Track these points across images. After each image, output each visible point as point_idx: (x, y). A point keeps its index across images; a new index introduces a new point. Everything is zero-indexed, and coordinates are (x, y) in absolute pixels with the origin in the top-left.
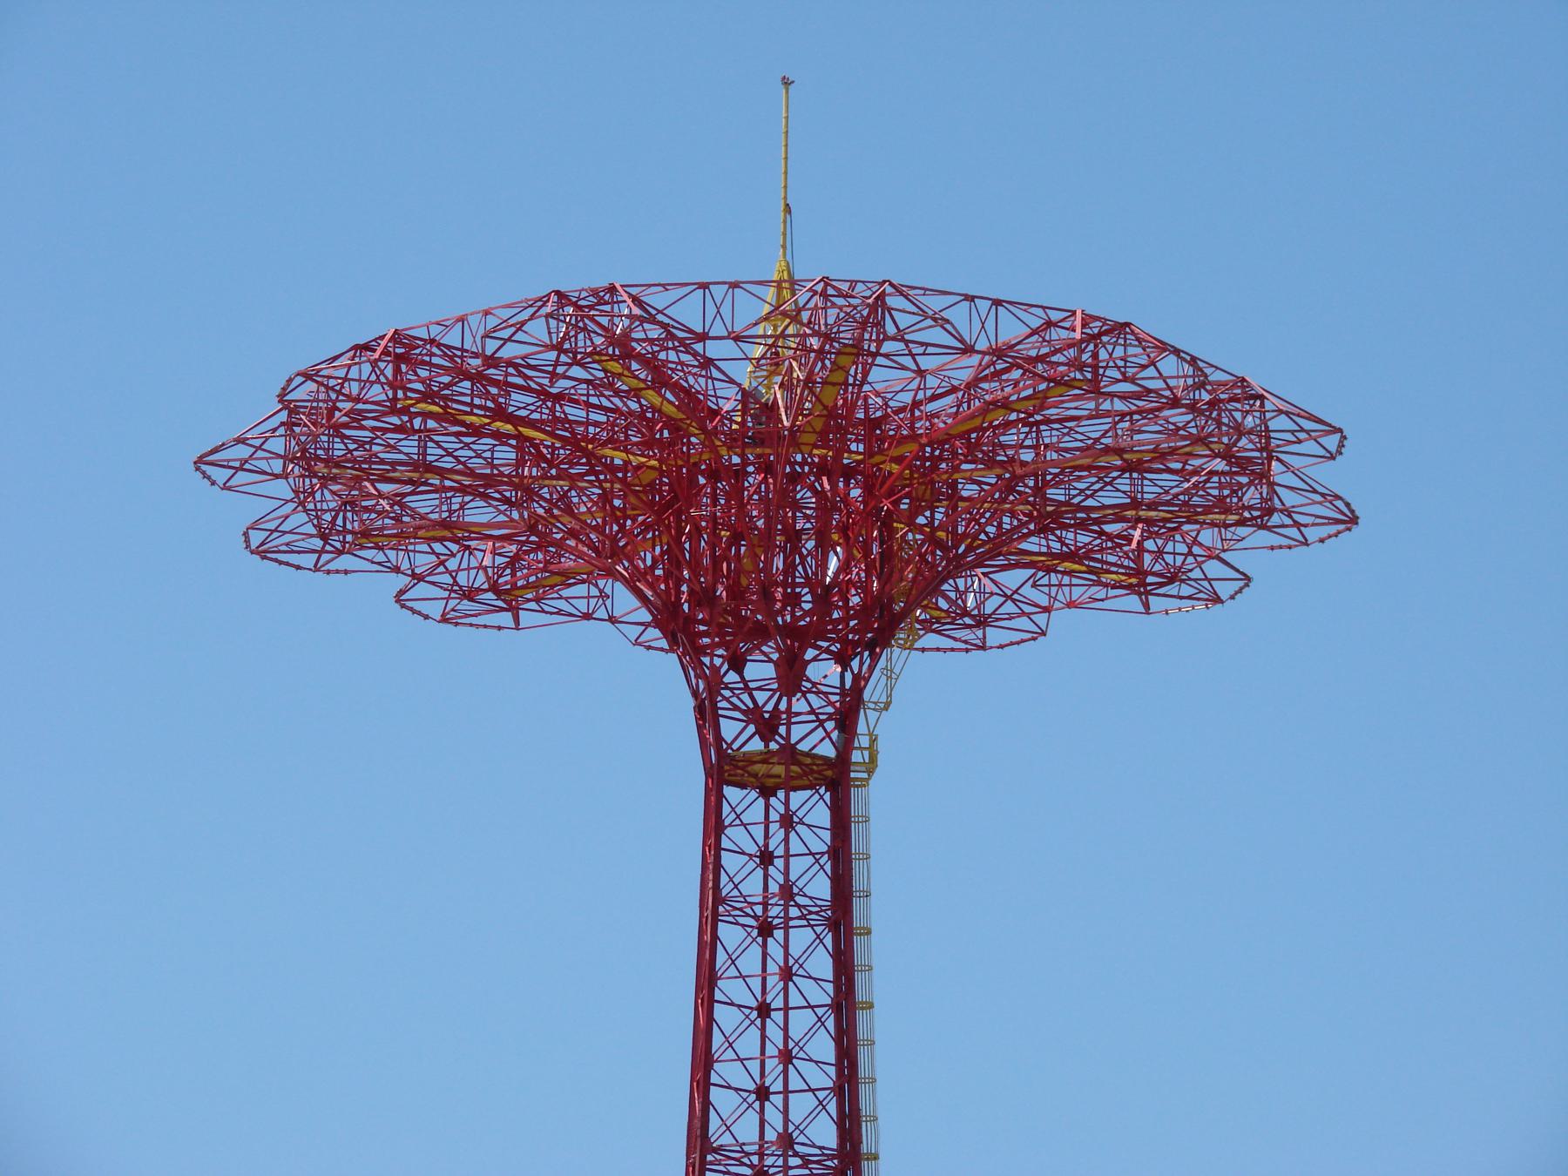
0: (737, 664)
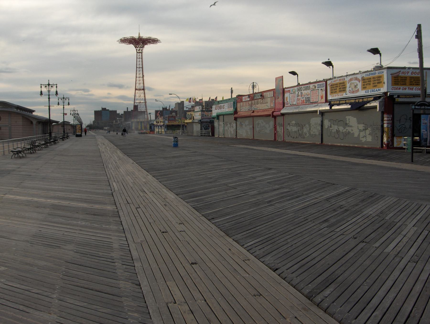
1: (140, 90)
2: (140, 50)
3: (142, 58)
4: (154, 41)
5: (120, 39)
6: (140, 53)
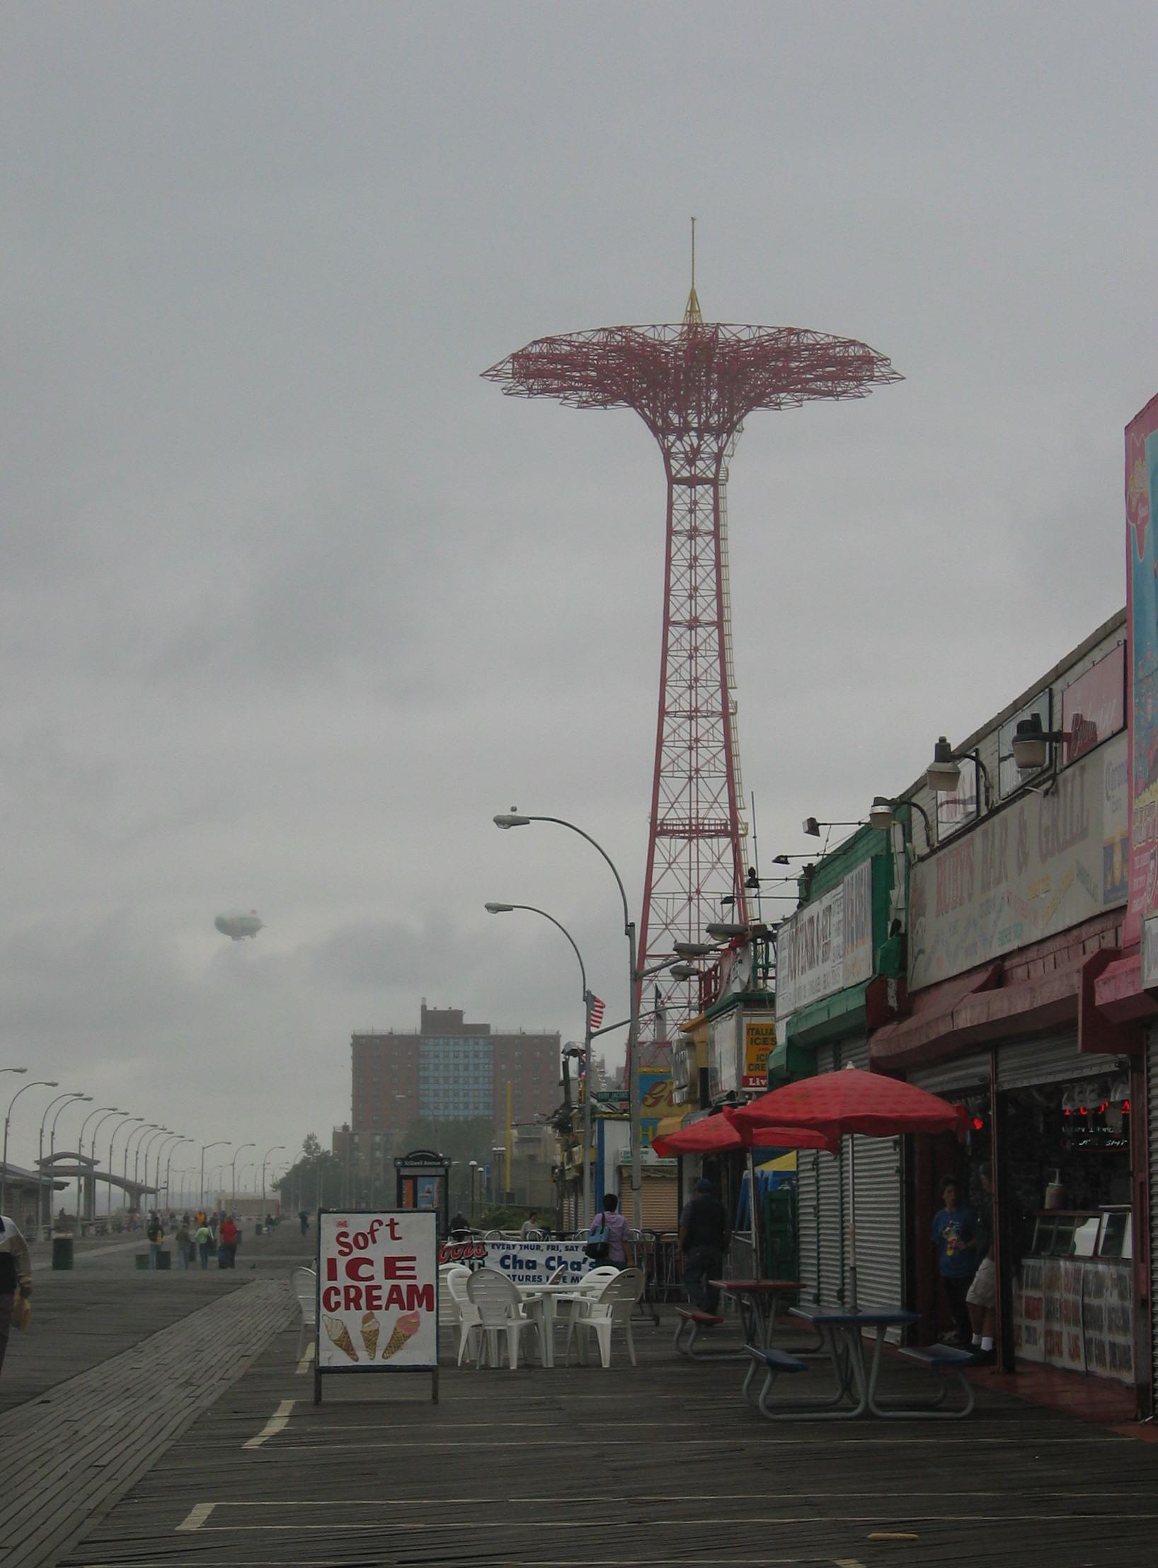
0: (680, 438)
1: (694, 832)
5: (515, 357)
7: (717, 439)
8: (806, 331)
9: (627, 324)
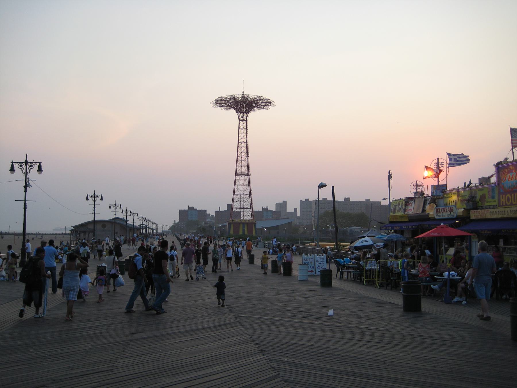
0: (240, 114)
1: (242, 175)
2: (243, 115)
3: (246, 129)
4: (266, 103)
5: (215, 100)
6: (244, 122)
7: (246, 114)
8: (262, 97)
9: (234, 94)
